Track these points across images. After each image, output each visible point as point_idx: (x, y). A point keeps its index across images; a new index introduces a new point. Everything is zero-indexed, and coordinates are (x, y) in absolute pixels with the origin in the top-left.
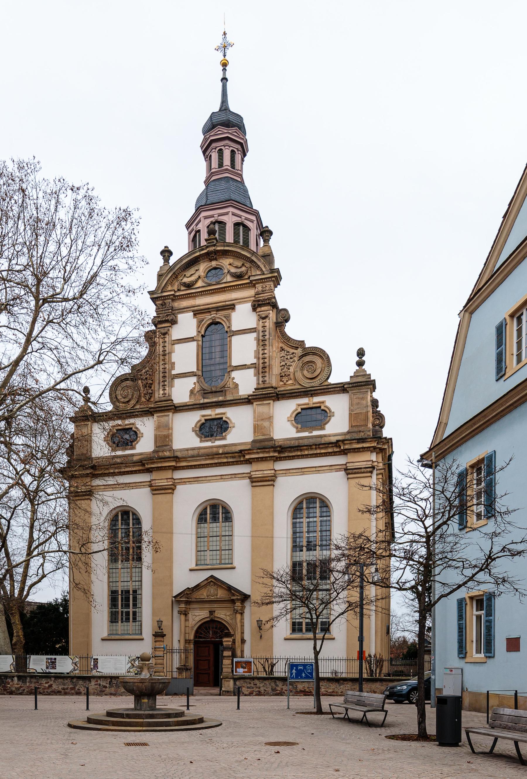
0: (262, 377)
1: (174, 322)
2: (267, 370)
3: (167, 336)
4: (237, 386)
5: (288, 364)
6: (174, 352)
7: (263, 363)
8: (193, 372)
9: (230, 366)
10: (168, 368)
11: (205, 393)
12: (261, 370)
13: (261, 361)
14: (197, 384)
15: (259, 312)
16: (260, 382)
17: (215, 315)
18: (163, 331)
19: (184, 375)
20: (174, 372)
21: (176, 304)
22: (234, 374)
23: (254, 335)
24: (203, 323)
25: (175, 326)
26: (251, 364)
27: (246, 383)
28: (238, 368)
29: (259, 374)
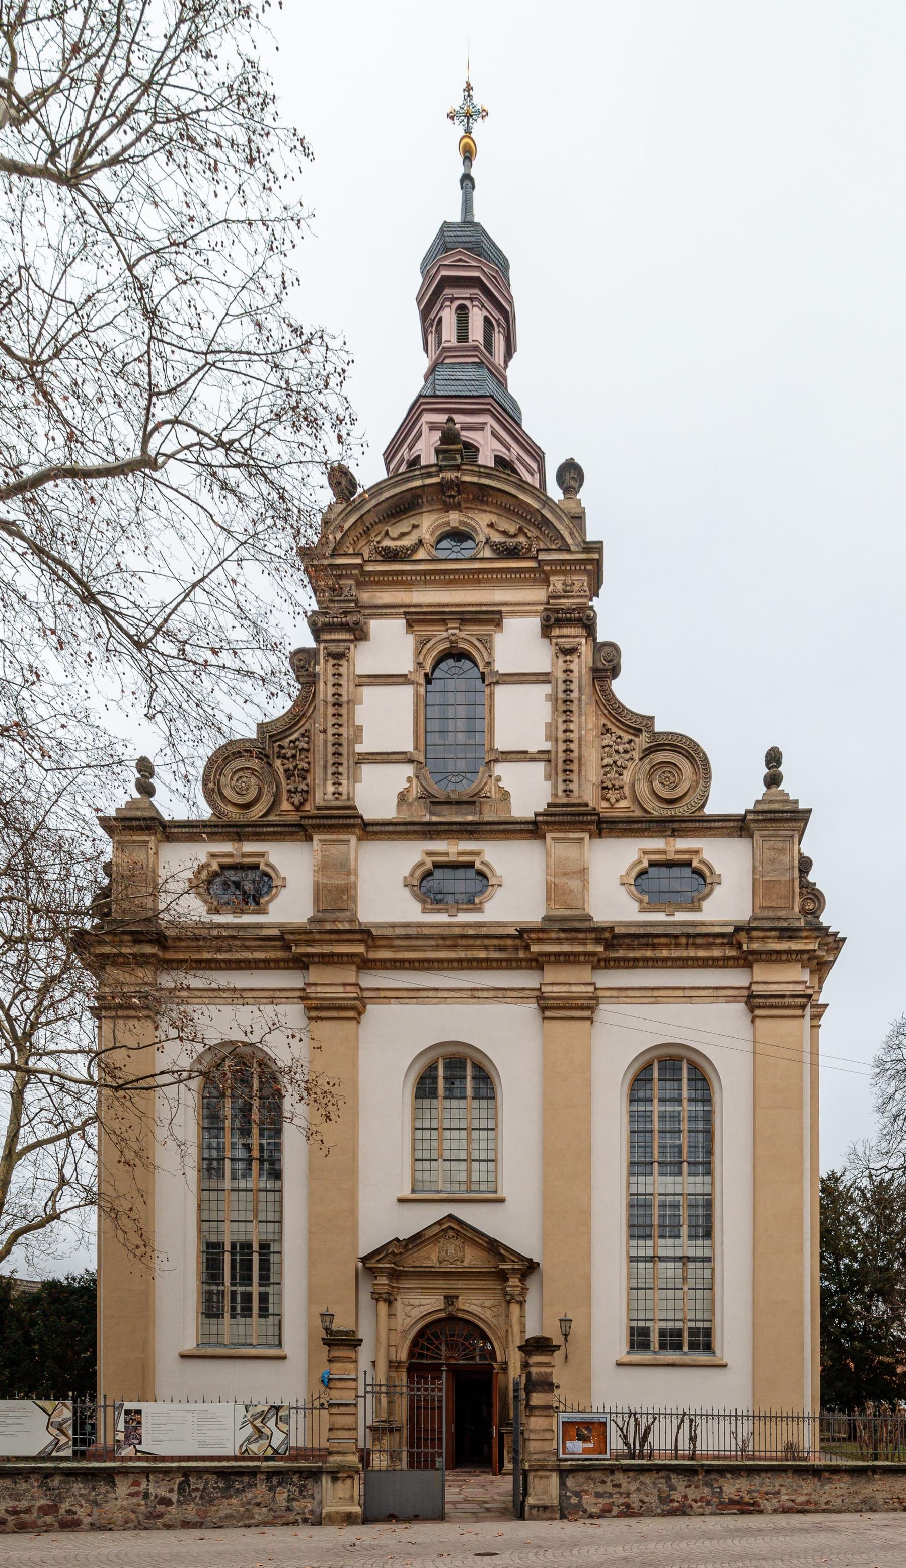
0: (565, 781)
1: (360, 634)
2: (575, 767)
3: (343, 662)
4: (506, 795)
5: (619, 763)
6: (361, 703)
7: (565, 751)
8: (405, 753)
9: (492, 749)
10: (345, 735)
11: (433, 802)
12: (561, 767)
13: (562, 747)
14: (415, 781)
15: (558, 637)
16: (560, 793)
17: (457, 631)
18: (333, 648)
19: (385, 757)
20: (359, 748)
21: (366, 596)
22: (499, 769)
23: (547, 689)
24: (429, 645)
25: (362, 645)
26: (540, 752)
27: (527, 791)
28: (509, 757)
29: (557, 774)
